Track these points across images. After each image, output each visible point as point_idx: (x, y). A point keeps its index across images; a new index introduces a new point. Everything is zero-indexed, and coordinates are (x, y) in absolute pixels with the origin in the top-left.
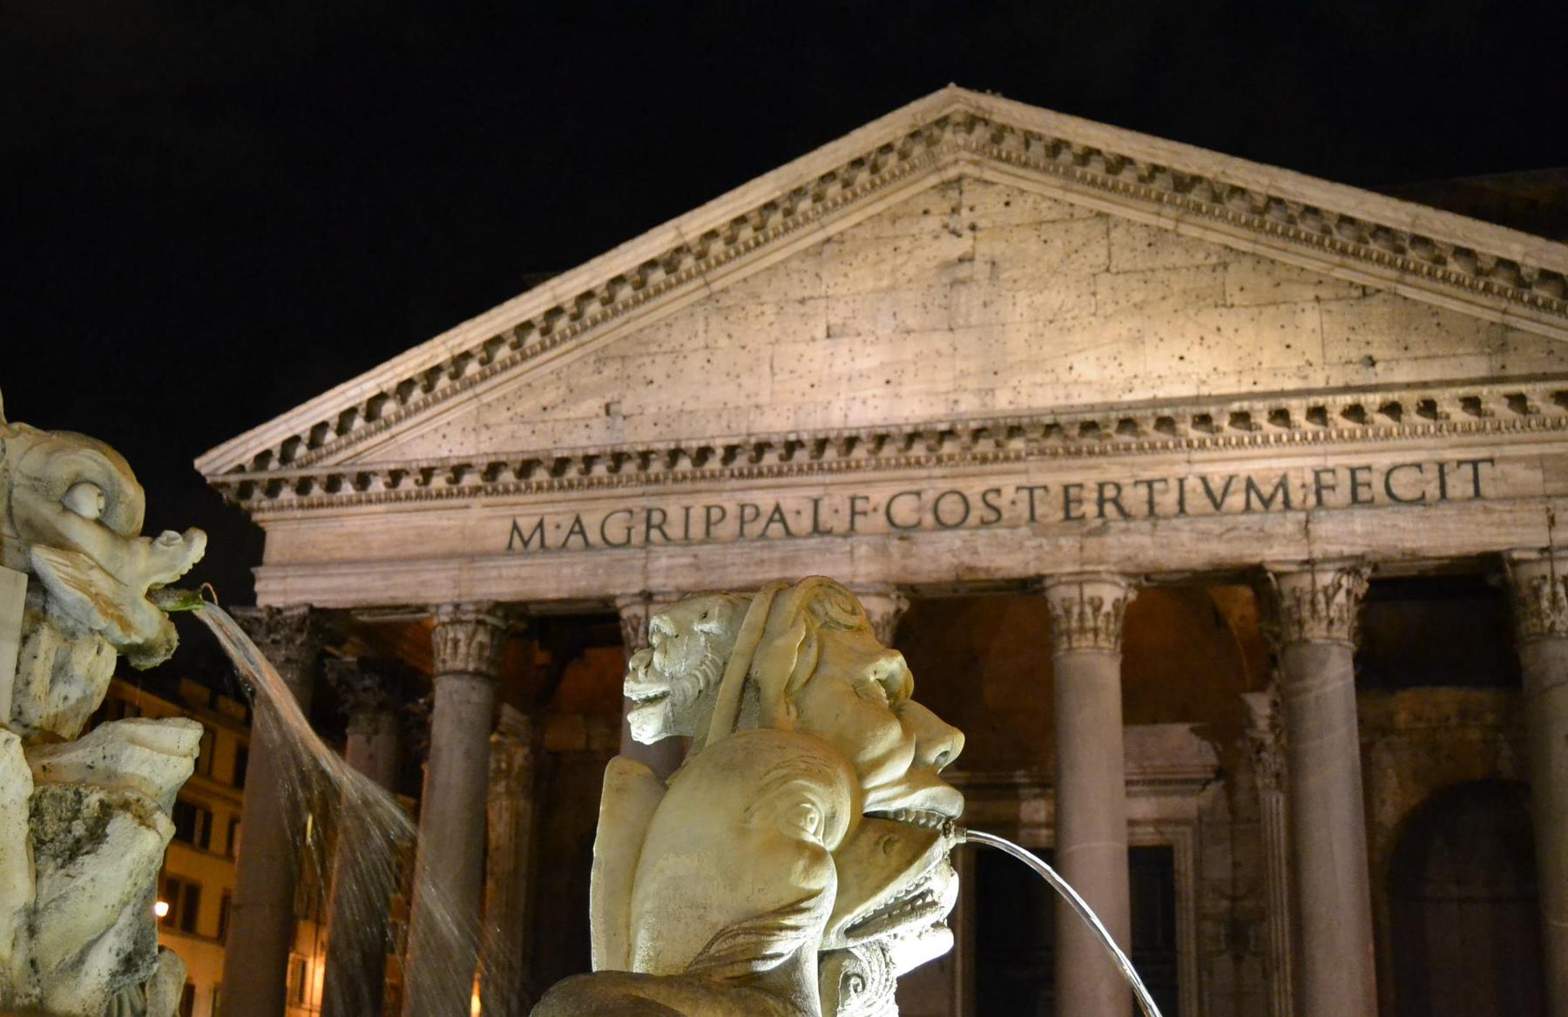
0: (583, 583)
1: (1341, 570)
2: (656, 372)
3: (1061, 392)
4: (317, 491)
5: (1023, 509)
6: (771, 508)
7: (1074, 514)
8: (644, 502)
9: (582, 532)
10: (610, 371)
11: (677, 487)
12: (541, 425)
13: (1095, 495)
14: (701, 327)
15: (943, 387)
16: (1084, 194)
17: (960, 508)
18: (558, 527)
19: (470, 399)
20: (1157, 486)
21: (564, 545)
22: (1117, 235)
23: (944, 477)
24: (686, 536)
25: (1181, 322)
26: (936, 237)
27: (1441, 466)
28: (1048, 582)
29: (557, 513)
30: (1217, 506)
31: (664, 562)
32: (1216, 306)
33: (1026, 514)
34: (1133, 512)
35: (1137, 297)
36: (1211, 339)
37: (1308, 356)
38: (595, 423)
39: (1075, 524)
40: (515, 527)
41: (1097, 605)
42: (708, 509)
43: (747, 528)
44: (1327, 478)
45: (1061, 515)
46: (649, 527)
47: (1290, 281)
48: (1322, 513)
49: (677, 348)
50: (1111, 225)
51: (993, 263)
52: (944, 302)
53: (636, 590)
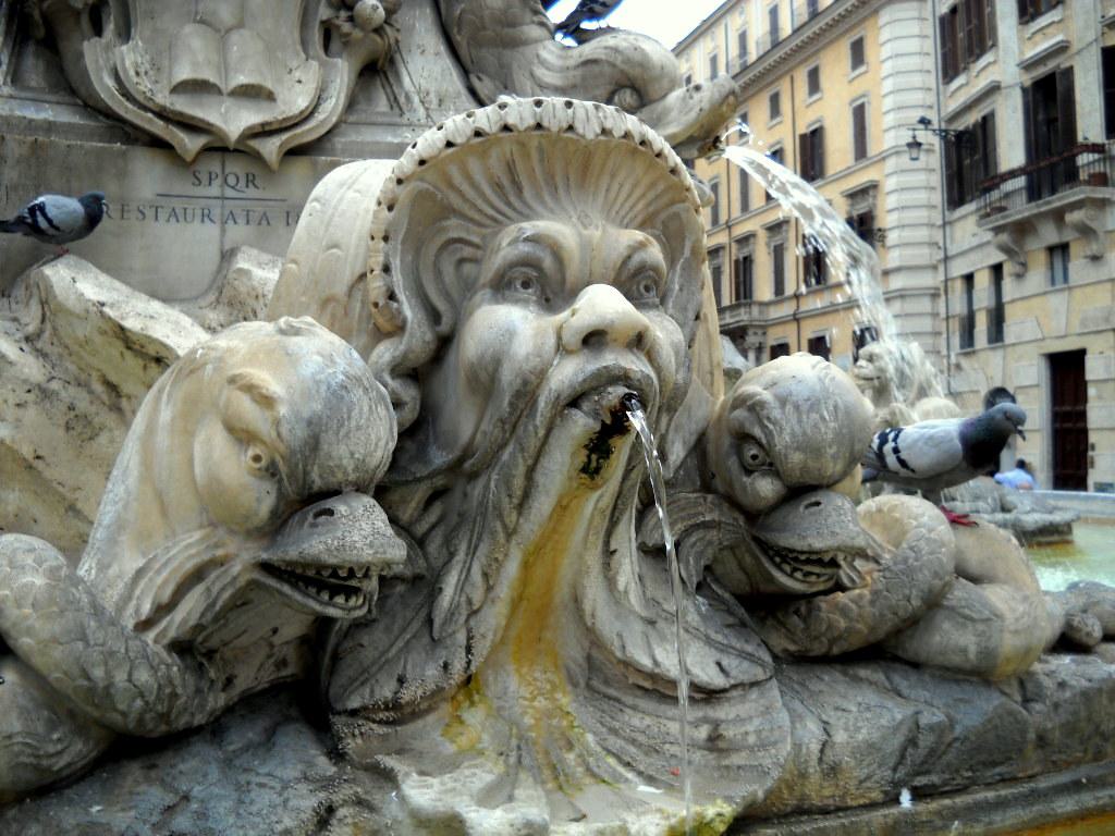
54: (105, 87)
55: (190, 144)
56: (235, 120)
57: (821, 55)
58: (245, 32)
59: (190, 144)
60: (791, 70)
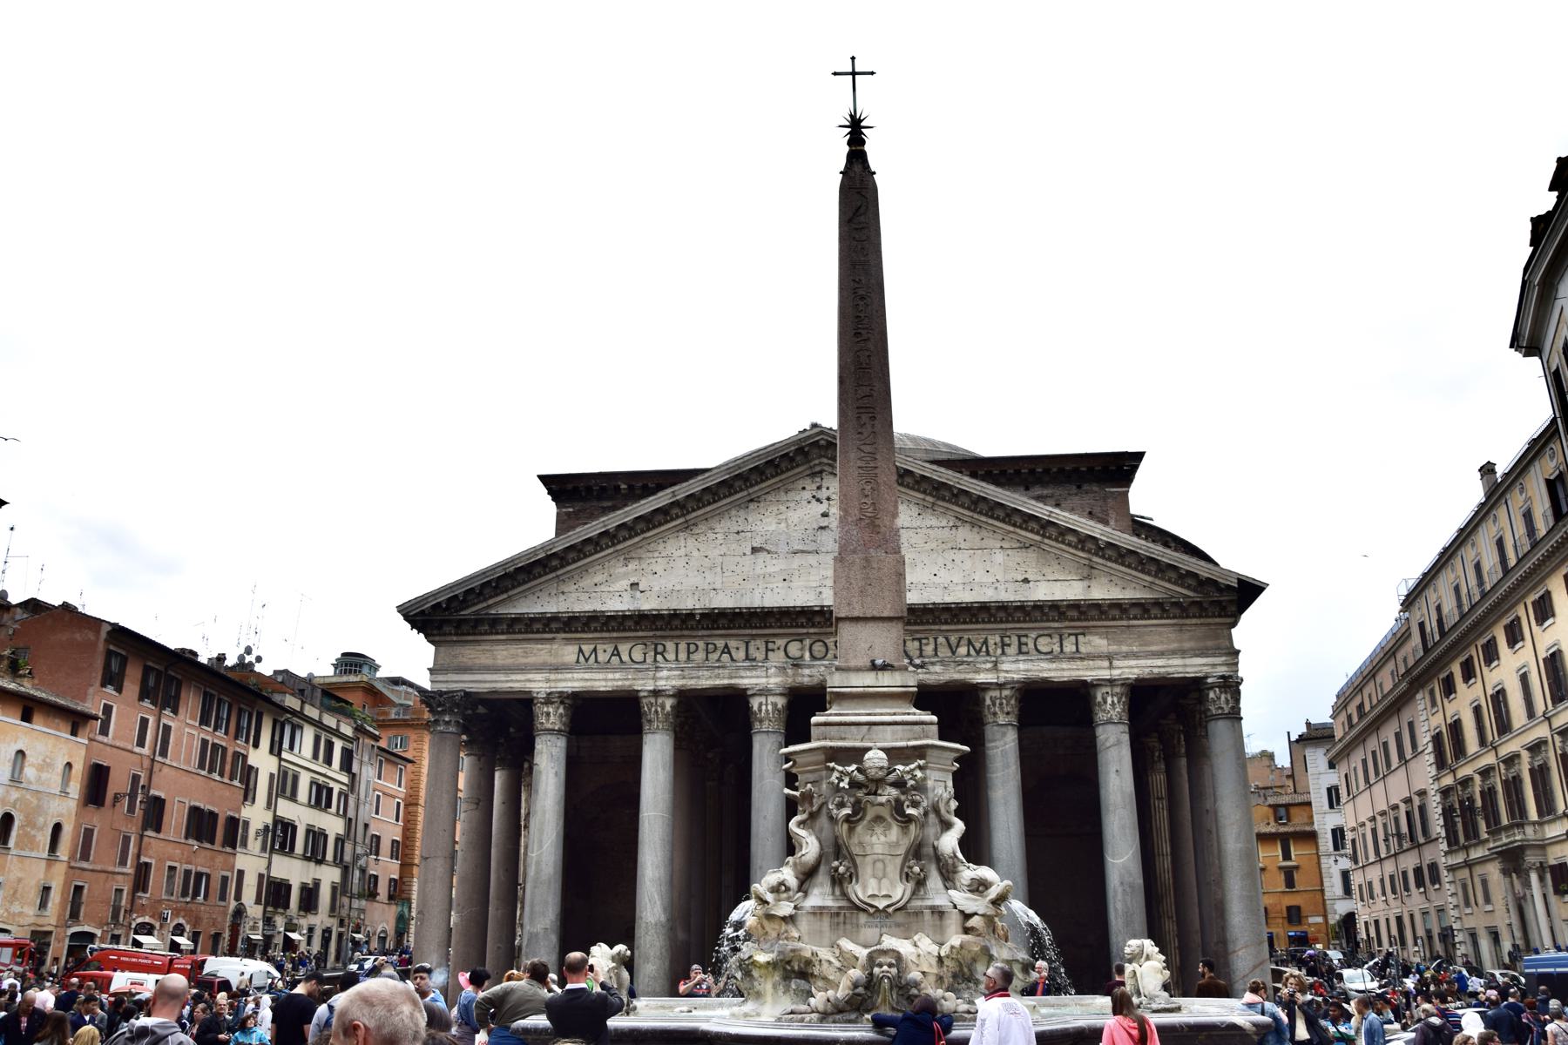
0: (620, 683)
2: (659, 568)
4: (465, 628)
9: (619, 655)
10: (632, 566)
15: (814, 584)
17: (824, 650)
20: (924, 641)
21: (609, 662)
23: (815, 633)
24: (677, 660)
26: (809, 502)
27: (1061, 636)
30: (954, 653)
31: (665, 673)
35: (913, 541)
38: (623, 594)
40: (581, 650)
42: (688, 644)
44: (1007, 640)
46: (656, 653)
48: (1004, 658)
52: (814, 538)
53: (651, 688)
55: (872, 910)
56: (881, 904)
57: (1547, 581)
59: (872, 910)
60: (1524, 597)
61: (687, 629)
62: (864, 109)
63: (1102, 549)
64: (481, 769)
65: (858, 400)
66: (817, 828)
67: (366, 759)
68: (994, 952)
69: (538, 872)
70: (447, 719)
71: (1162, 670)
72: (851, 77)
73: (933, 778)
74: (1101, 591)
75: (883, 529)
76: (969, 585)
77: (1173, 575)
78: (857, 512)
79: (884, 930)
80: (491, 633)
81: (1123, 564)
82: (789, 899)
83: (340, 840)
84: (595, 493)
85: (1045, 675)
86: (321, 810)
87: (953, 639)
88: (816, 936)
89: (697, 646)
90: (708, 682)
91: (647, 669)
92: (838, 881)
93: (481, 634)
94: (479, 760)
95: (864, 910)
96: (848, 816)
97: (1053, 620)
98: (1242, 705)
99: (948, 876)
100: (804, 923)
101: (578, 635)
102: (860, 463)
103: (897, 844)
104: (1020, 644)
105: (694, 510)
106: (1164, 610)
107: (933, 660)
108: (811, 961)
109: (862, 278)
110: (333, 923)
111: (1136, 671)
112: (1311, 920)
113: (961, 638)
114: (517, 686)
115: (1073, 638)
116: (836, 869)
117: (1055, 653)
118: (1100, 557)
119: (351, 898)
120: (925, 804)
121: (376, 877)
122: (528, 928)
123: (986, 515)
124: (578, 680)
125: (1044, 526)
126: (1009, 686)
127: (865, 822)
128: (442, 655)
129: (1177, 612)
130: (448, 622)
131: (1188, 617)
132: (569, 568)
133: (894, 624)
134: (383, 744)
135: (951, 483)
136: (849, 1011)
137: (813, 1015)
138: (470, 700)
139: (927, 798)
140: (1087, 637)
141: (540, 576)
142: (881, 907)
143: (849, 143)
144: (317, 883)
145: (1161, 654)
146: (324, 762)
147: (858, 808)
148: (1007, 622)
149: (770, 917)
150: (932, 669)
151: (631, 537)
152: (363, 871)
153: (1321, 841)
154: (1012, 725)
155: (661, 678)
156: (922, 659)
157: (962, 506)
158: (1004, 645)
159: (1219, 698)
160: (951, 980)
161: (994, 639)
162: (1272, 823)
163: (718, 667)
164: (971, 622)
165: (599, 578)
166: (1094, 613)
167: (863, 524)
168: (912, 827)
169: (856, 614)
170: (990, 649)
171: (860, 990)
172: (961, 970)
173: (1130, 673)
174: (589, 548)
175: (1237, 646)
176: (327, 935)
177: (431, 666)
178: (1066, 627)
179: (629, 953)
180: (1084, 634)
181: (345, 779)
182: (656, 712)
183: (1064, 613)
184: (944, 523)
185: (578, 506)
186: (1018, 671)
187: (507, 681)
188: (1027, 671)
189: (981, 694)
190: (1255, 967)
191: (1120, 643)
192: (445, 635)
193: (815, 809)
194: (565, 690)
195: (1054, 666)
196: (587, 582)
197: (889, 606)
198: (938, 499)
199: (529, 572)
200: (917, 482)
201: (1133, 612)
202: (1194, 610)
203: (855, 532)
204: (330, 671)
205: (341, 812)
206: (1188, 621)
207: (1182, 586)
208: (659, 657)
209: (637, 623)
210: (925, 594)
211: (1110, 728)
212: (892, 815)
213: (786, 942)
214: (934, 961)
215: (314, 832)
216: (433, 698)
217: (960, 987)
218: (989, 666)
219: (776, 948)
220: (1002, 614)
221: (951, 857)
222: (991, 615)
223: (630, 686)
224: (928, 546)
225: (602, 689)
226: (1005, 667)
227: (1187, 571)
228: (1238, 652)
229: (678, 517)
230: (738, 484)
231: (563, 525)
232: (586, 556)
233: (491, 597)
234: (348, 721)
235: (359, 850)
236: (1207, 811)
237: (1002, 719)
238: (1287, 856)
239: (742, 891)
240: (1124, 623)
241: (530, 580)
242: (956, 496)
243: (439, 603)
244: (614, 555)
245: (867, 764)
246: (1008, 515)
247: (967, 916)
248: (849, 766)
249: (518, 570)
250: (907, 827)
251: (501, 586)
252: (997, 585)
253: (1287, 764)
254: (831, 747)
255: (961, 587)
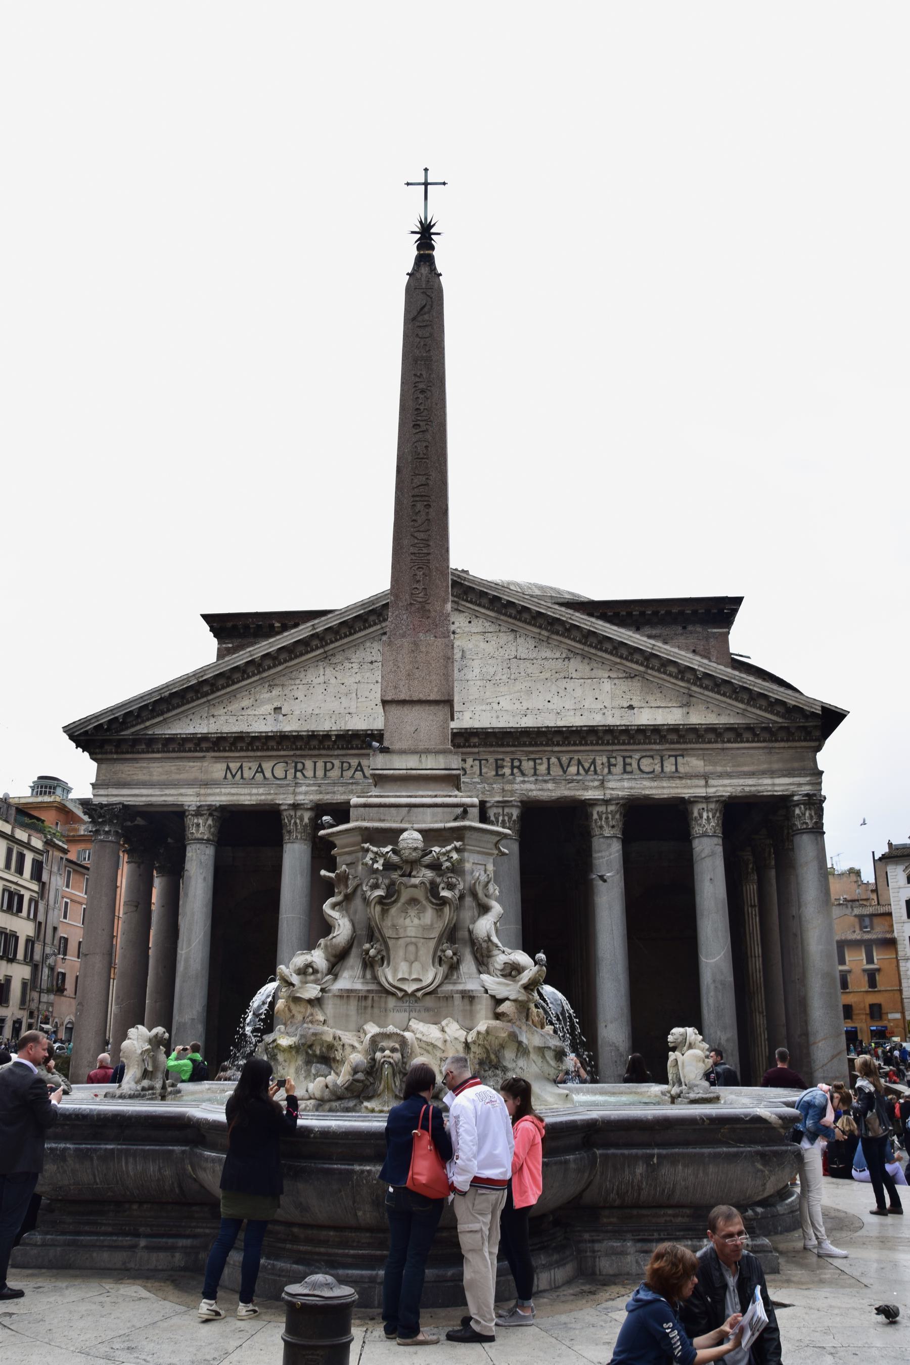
0: (263, 797)
1: (617, 804)
2: (300, 694)
3: (494, 715)
4: (124, 747)
5: (476, 769)
6: (356, 764)
7: (500, 773)
8: (294, 759)
9: (262, 772)
10: (275, 692)
11: (311, 752)
12: (241, 717)
13: (509, 764)
14: (322, 673)
16: (506, 622)
18: (250, 769)
19: (205, 702)
20: (538, 761)
21: (253, 778)
22: (520, 641)
24: (315, 776)
25: (549, 684)
28: (488, 805)
29: (250, 762)
30: (565, 772)
31: (303, 789)
32: (565, 678)
33: (478, 772)
34: (526, 773)
35: (529, 671)
36: (562, 693)
37: (605, 704)
38: (268, 717)
39: (500, 777)
40: (228, 768)
41: (510, 816)
42: (325, 763)
43: (344, 773)
44: (613, 761)
45: (494, 773)
46: (296, 771)
47: (598, 668)
48: (610, 777)
49: (310, 682)
50: (518, 636)
51: (463, 651)
53: (291, 802)
54: (383, 981)
55: (400, 994)
56: (410, 988)
58: (416, 963)
59: (400, 994)
61: (324, 748)
62: (434, 215)
63: (700, 679)
64: (140, 875)
65: (414, 488)
66: (351, 911)
67: (55, 869)
68: (524, 1038)
69: (186, 968)
70: (107, 829)
71: (753, 789)
72: (423, 186)
73: (471, 861)
74: (698, 717)
75: (433, 614)
76: (579, 710)
77: (764, 703)
78: (408, 597)
79: (413, 1014)
80: (148, 752)
81: (718, 693)
82: (316, 982)
83: (30, 942)
84: (252, 631)
85: (647, 792)
86: (12, 914)
87: (564, 759)
88: (342, 1021)
89: (333, 765)
90: (342, 797)
91: (288, 785)
92: (369, 964)
93: (139, 753)
94: (139, 867)
95: (393, 994)
96: (381, 897)
97: (655, 743)
98: (825, 820)
99: (483, 959)
100: (330, 1006)
101: (227, 754)
102: (412, 550)
103: (431, 927)
104: (625, 764)
105: (332, 642)
106: (755, 735)
107: (545, 778)
108: (333, 1045)
109: (424, 373)
110: (23, 1015)
111: (729, 789)
112: (891, 1016)
113: (571, 759)
114: (170, 799)
115: (672, 760)
116: (367, 952)
117: (656, 773)
118: (698, 686)
119: (40, 992)
120: (461, 887)
121: (64, 975)
122: (177, 1018)
123: (596, 648)
124: (225, 794)
125: (647, 658)
126: (614, 802)
127: (399, 904)
128: (103, 772)
129: (767, 736)
130: (109, 741)
131: (776, 741)
132: (219, 694)
133: (441, 707)
134: (72, 856)
135: (564, 619)
136: (349, 1098)
137: (308, 1102)
138: (127, 812)
139: (464, 881)
140: (686, 759)
141: (193, 701)
142: (410, 991)
143: (419, 248)
144: (8, 979)
145: (752, 774)
146: (16, 871)
147: (392, 892)
148: (613, 744)
149: (297, 1000)
150: (546, 786)
151: (275, 666)
152: (52, 969)
153: (900, 947)
154: (617, 837)
155: (300, 793)
156: (535, 777)
157: (574, 640)
158: (610, 765)
159: (804, 814)
160: (477, 1067)
161: (601, 760)
162: (858, 931)
163: (352, 783)
164: (581, 744)
165: (245, 703)
166: (692, 736)
167: (413, 608)
168: (447, 910)
169: (402, 697)
170: (597, 769)
171: (360, 1076)
172: (488, 1057)
173: (724, 791)
174: (237, 676)
175: (820, 768)
176: (17, 1025)
177: (93, 781)
178: (667, 749)
179: (167, 1035)
180: (683, 756)
181: (35, 887)
182: (295, 823)
183: (665, 736)
184: (558, 655)
185: (237, 642)
186: (623, 789)
187: (162, 795)
188: (631, 788)
189: (589, 810)
190: (833, 1057)
191: (715, 764)
192: (106, 753)
193: (349, 891)
194: (214, 803)
195: (655, 784)
196: (235, 706)
197: (436, 689)
198: (553, 633)
199: (183, 697)
200: (534, 618)
201: (728, 735)
202: (782, 734)
203: (405, 617)
204: (28, 792)
205: (32, 916)
206: (776, 745)
207: (772, 713)
208: (299, 774)
209: (279, 743)
210: (539, 718)
211: (705, 840)
212: (427, 898)
213: (310, 1025)
214: (461, 1047)
215: (6, 934)
216: (95, 810)
217: (486, 1074)
218: (596, 783)
219: (299, 1032)
220: (608, 737)
221: (485, 941)
222: (599, 738)
223: (272, 800)
224: (543, 676)
225: (247, 803)
226: (611, 785)
227: (776, 699)
228: (822, 773)
229: (317, 648)
230: (372, 618)
231: (221, 655)
232: (234, 683)
233: (148, 719)
234: (39, 835)
235: (48, 950)
236: (793, 916)
237: (607, 832)
238: (870, 960)
239: (268, 972)
240: (719, 746)
241: (183, 705)
242: (568, 630)
243: (101, 725)
244: (260, 682)
245: (402, 844)
246: (615, 648)
247: (498, 1002)
248: (385, 847)
249: (173, 695)
250: (441, 910)
251: (157, 709)
252: (605, 711)
253: (872, 881)
254: (367, 828)
255: (572, 713)
